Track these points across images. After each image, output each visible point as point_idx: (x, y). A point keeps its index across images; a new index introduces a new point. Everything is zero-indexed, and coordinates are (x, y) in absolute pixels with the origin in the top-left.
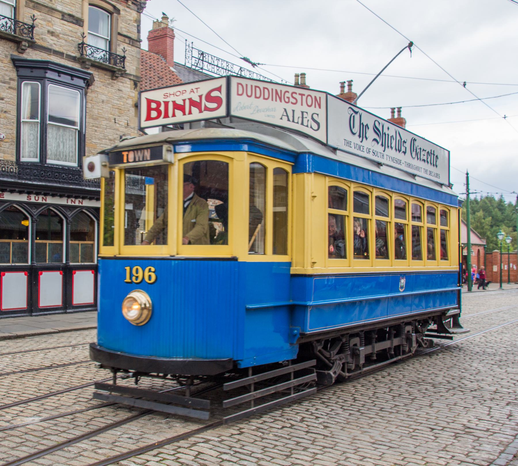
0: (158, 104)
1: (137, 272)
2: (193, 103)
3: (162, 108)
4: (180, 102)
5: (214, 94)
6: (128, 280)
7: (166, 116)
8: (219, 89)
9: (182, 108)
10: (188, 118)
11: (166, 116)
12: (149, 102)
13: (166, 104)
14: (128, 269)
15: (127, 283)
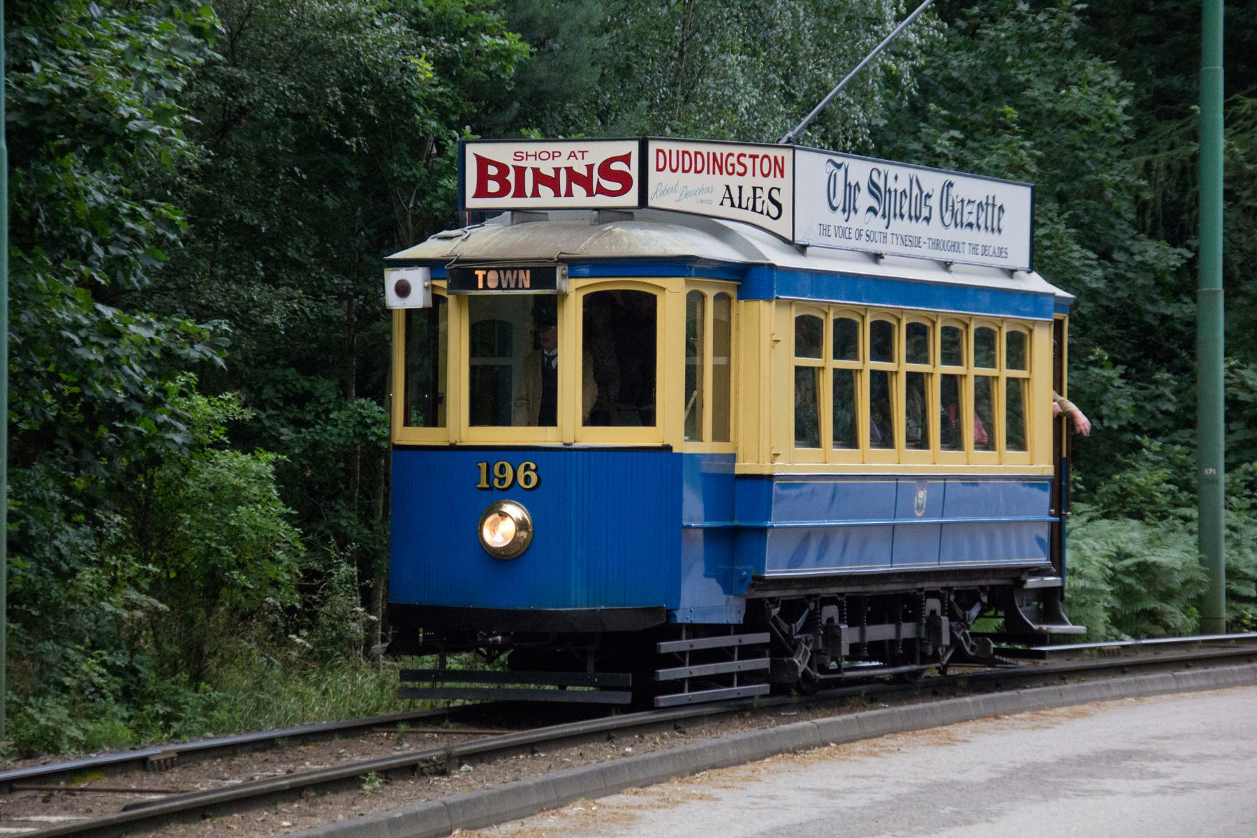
0: (503, 169)
2: (573, 176)
3: (511, 178)
7: (520, 193)
8: (626, 159)
9: (553, 183)
11: (520, 193)
12: (483, 163)
13: (520, 171)
14: (483, 466)
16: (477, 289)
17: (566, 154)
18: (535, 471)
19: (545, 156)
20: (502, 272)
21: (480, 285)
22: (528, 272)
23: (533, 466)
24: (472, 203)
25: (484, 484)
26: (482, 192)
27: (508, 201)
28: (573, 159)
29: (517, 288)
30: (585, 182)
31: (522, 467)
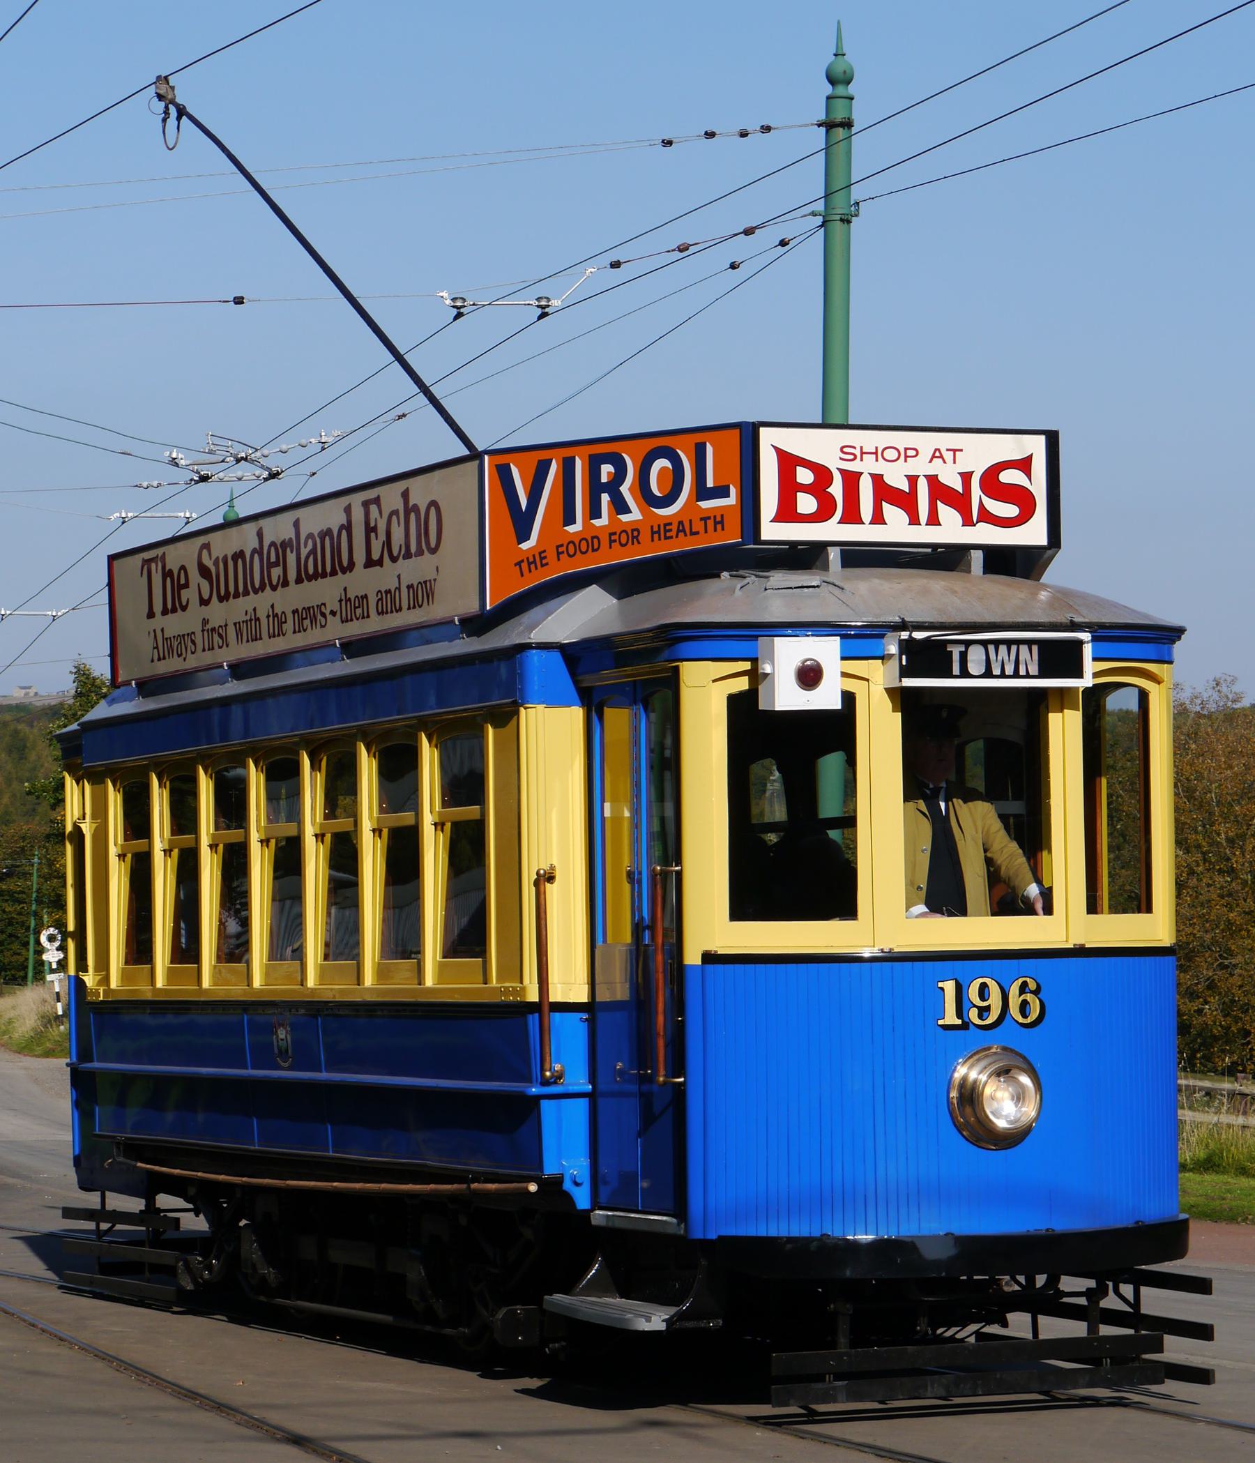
0: (823, 475)
1: (983, 991)
3: (836, 489)
4: (896, 478)
5: (1010, 477)
6: (951, 1018)
7: (852, 516)
8: (1024, 465)
9: (906, 501)
10: (924, 534)
11: (852, 516)
12: (788, 463)
13: (851, 480)
14: (949, 987)
15: (942, 1026)
16: (950, 675)
17: (926, 453)
18: (1036, 992)
19: (890, 454)
20: (991, 648)
21: (956, 670)
22: (1035, 648)
23: (1032, 986)
24: (771, 531)
25: (951, 1018)
26: (787, 513)
27: (832, 530)
28: (938, 461)
29: (1016, 675)
30: (960, 501)
31: (1014, 990)
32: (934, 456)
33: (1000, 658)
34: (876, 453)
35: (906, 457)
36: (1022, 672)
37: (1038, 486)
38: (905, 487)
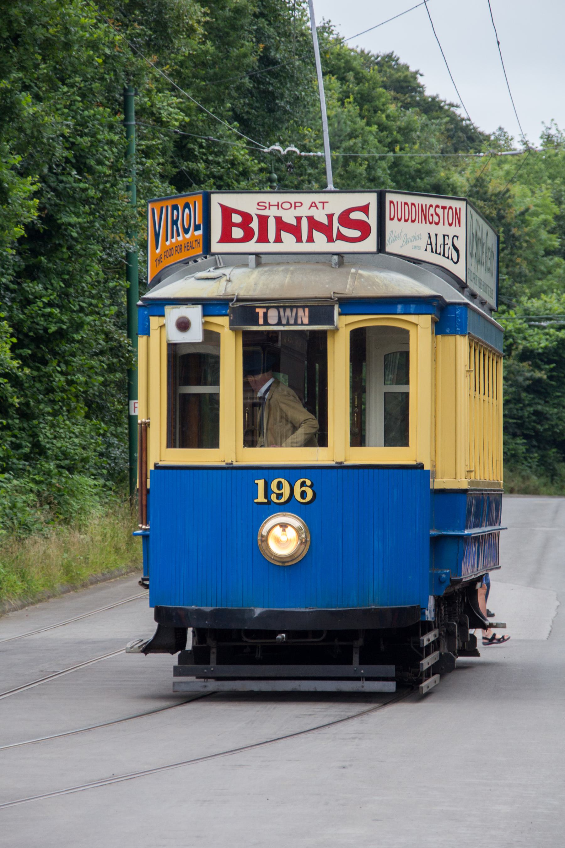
0: (247, 218)
3: (255, 225)
4: (289, 218)
5: (355, 216)
7: (263, 238)
8: (365, 209)
9: (295, 231)
11: (263, 238)
12: (227, 212)
13: (263, 220)
16: (257, 323)
17: (307, 204)
19: (287, 206)
20: (281, 310)
21: (261, 321)
22: (307, 310)
25: (261, 498)
26: (226, 237)
28: (314, 209)
29: (296, 324)
30: (326, 230)
32: (311, 206)
33: (286, 314)
34: (278, 205)
35: (295, 207)
36: (299, 322)
37: (372, 220)
38: (294, 223)
